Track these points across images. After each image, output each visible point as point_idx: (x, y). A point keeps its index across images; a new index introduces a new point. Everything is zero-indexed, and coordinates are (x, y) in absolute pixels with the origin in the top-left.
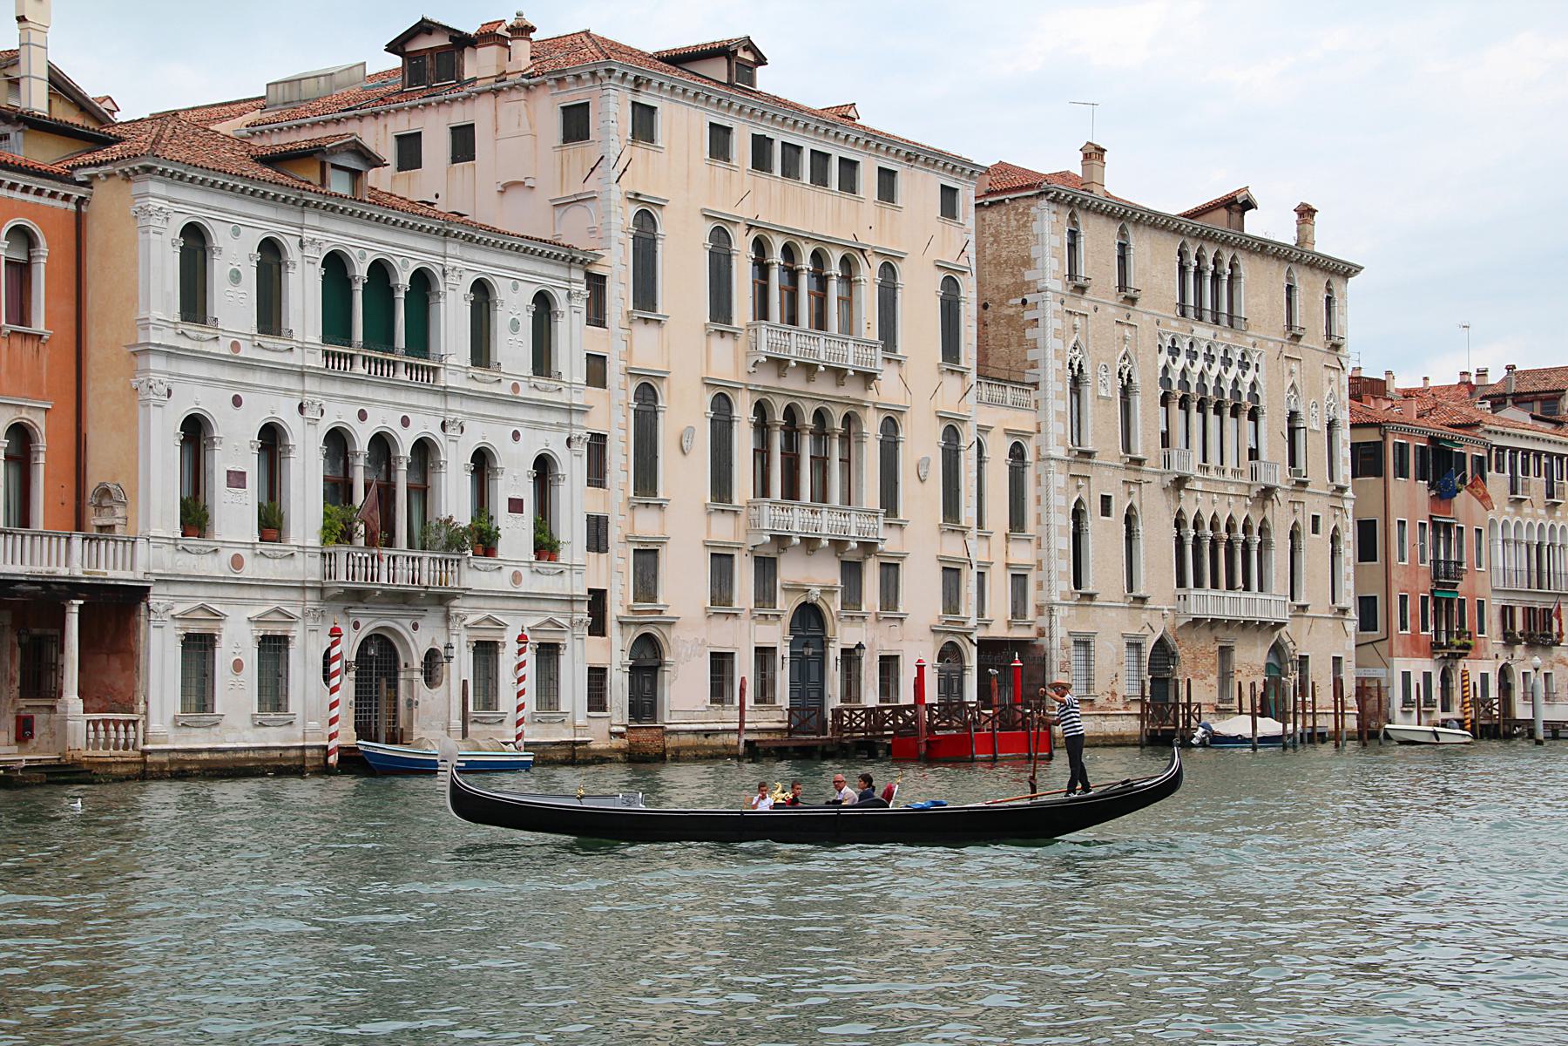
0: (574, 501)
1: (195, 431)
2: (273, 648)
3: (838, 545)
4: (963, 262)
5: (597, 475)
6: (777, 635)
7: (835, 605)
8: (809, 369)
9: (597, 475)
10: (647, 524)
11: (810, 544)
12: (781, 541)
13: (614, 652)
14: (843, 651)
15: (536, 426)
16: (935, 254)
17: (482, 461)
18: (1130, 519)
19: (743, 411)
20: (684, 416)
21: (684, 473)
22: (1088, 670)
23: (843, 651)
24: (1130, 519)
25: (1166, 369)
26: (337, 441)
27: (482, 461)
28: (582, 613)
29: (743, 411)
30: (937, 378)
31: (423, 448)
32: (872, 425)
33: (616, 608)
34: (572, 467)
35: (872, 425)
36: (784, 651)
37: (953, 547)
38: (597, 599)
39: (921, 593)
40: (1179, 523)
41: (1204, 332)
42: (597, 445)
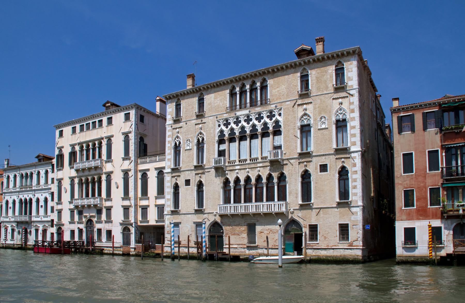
0: (50, 204)
1: (7, 202)
2: (13, 230)
3: (95, 206)
4: (131, 130)
5: (53, 200)
6: (82, 226)
7: (95, 220)
8: (90, 169)
9: (53, 200)
10: (59, 207)
11: (89, 206)
12: (83, 206)
13: (54, 230)
14: (98, 229)
15: (44, 193)
16: (123, 131)
17: (38, 200)
18: (200, 185)
19: (76, 181)
20: (66, 184)
21: (66, 197)
22: (197, 233)
23: (98, 229)
24: (200, 185)
25: (222, 131)
26: (21, 200)
27: (38, 200)
28: (50, 224)
29: (76, 181)
30: (122, 162)
31: (31, 200)
32: (104, 177)
33: (55, 223)
34: (49, 199)
35: (104, 177)
36: (84, 230)
37: (126, 203)
38: (53, 221)
39: (118, 215)
40: (226, 182)
41: (242, 113)
42: (52, 194)
